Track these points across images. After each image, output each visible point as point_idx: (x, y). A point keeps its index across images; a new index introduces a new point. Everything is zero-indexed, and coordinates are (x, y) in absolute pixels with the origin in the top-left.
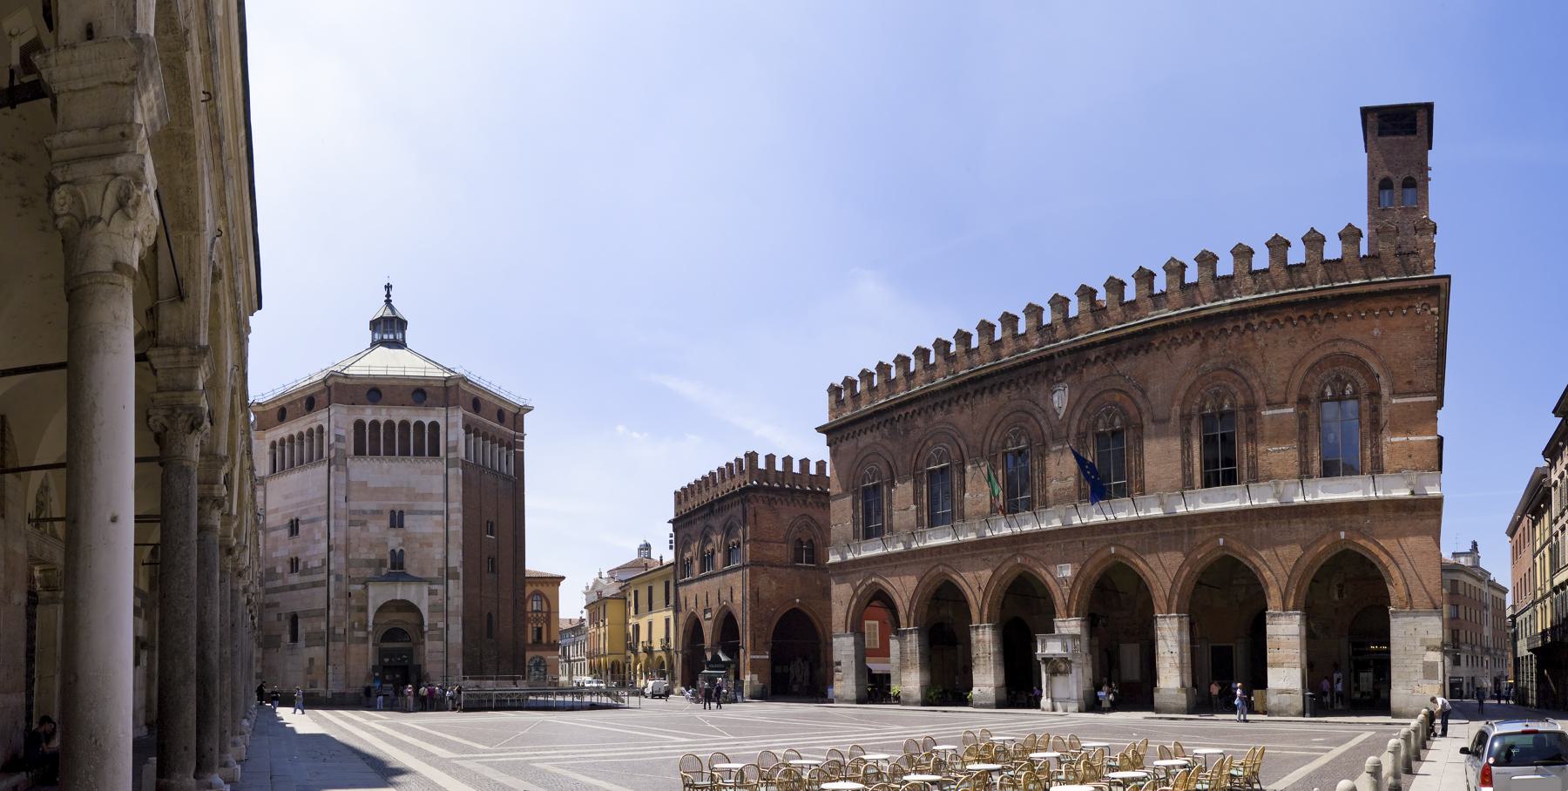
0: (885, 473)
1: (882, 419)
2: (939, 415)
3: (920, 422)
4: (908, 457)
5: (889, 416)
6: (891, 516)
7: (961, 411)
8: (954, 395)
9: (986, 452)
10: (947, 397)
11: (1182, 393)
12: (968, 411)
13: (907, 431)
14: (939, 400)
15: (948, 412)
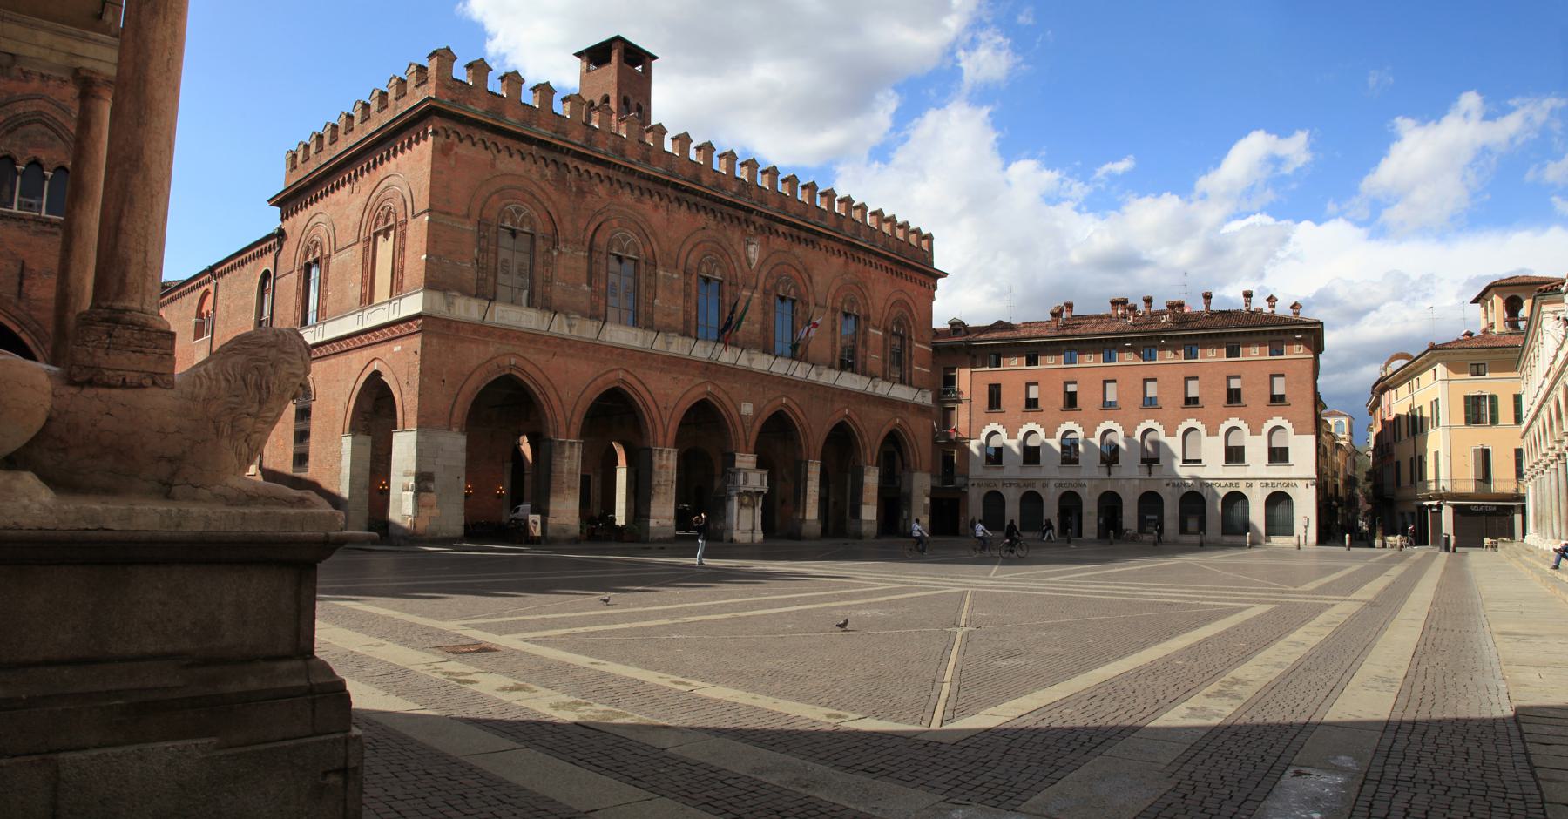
0: (542, 226)
1: (550, 156)
2: (627, 198)
3: (602, 190)
4: (582, 224)
5: (556, 156)
6: (549, 282)
7: (656, 207)
8: (650, 185)
9: (681, 262)
10: (643, 184)
11: (833, 291)
12: (662, 213)
13: (581, 192)
14: (634, 181)
15: (639, 200)
